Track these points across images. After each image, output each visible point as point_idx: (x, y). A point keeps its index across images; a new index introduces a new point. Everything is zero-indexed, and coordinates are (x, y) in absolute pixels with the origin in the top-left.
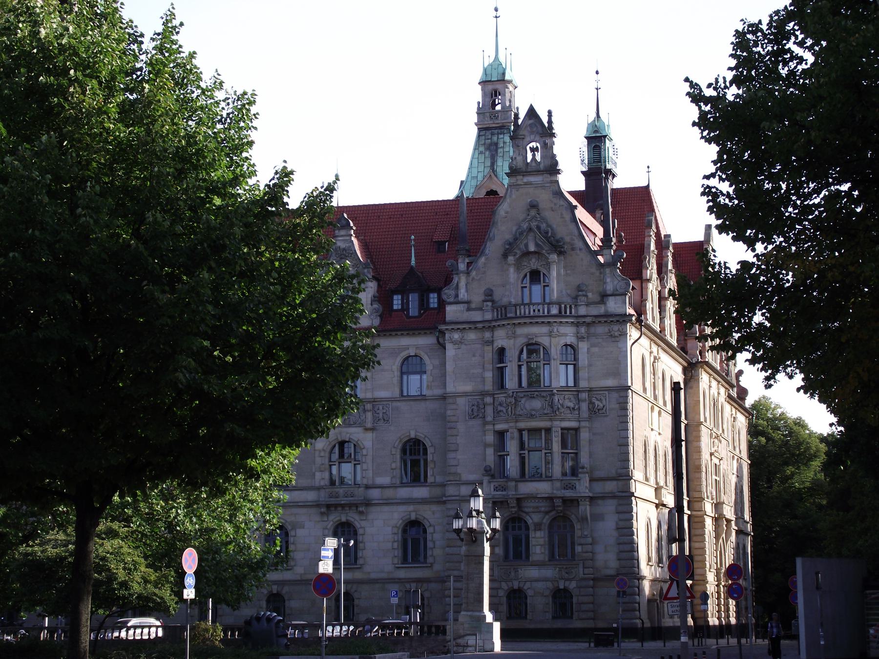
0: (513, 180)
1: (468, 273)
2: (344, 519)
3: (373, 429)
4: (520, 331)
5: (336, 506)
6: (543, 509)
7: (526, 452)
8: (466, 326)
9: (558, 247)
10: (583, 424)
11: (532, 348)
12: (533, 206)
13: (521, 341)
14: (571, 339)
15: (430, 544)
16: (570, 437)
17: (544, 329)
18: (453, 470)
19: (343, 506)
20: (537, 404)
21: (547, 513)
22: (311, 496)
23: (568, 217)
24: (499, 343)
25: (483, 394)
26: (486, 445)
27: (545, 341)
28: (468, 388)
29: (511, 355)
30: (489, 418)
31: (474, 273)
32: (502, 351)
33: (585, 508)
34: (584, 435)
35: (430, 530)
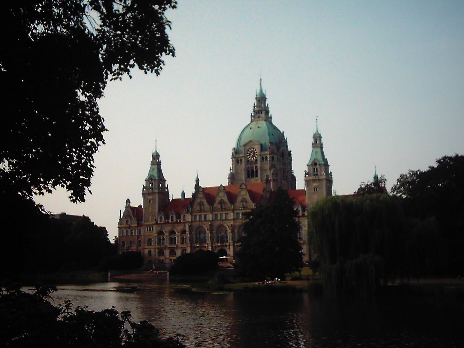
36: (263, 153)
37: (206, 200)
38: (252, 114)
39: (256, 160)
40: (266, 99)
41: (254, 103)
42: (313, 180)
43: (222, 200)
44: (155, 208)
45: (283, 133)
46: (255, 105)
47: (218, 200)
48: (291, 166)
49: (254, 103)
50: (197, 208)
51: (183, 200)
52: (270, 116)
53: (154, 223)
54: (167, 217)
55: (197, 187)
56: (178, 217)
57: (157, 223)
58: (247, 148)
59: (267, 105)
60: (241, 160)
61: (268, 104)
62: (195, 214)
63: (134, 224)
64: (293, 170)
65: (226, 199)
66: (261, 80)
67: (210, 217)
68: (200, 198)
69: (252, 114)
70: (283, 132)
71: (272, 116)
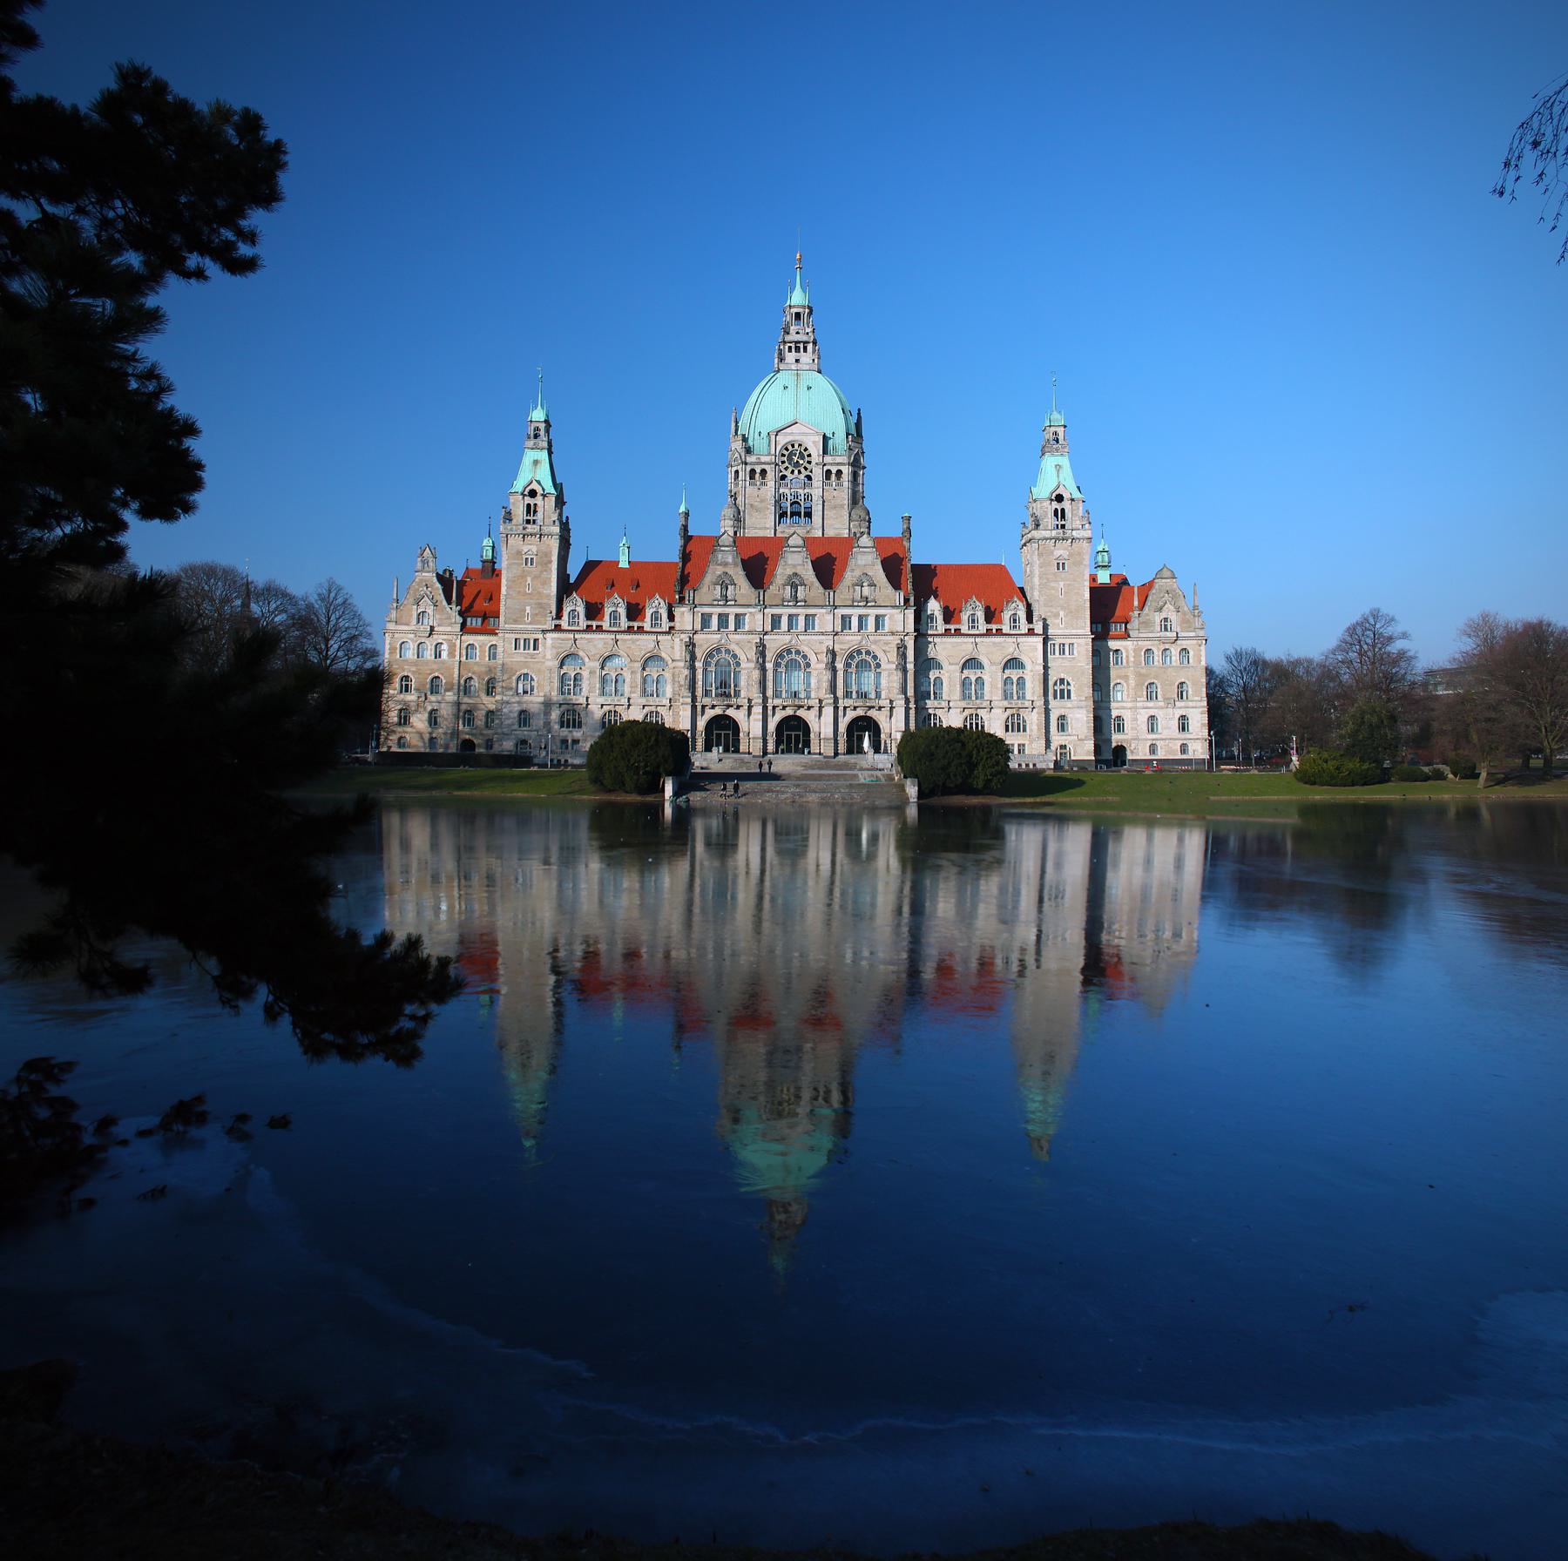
36: (828, 459)
37: (742, 573)
39: (809, 478)
42: (1057, 539)
43: (796, 574)
44: (546, 582)
47: (782, 572)
50: (707, 591)
51: (624, 564)
53: (550, 625)
54: (593, 611)
55: (685, 528)
56: (635, 612)
57: (558, 628)
58: (783, 440)
60: (764, 472)
62: (707, 610)
63: (451, 624)
65: (809, 574)
67: (756, 620)
68: (726, 564)
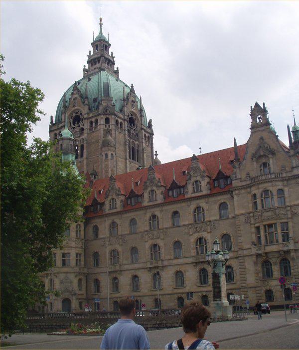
0: (253, 130)
1: (239, 168)
2: (202, 268)
3: (210, 232)
4: (260, 186)
5: (199, 262)
6: (276, 256)
7: (267, 234)
8: (240, 188)
9: (273, 153)
10: (289, 220)
11: (266, 191)
12: (261, 138)
13: (261, 190)
14: (280, 187)
15: (235, 275)
16: (285, 225)
17: (270, 184)
18: (240, 244)
19: (201, 262)
20: (270, 213)
21: (278, 258)
22: (190, 260)
23: (275, 139)
24: (253, 192)
25: (249, 213)
26: (252, 233)
27: (271, 188)
28: (243, 212)
29: (258, 196)
30: (252, 222)
31: (241, 167)
32: (255, 195)
33: (293, 254)
34: (290, 224)
35: (234, 269)
38: (85, 66)
39: (82, 129)
40: (110, 45)
41: (90, 51)
45: (132, 86)
46: (90, 53)
48: (152, 144)
49: (90, 51)
52: (116, 69)
59: (110, 54)
61: (112, 53)
64: (156, 152)
66: (101, 20)
69: (85, 66)
70: (132, 85)
71: (119, 69)
